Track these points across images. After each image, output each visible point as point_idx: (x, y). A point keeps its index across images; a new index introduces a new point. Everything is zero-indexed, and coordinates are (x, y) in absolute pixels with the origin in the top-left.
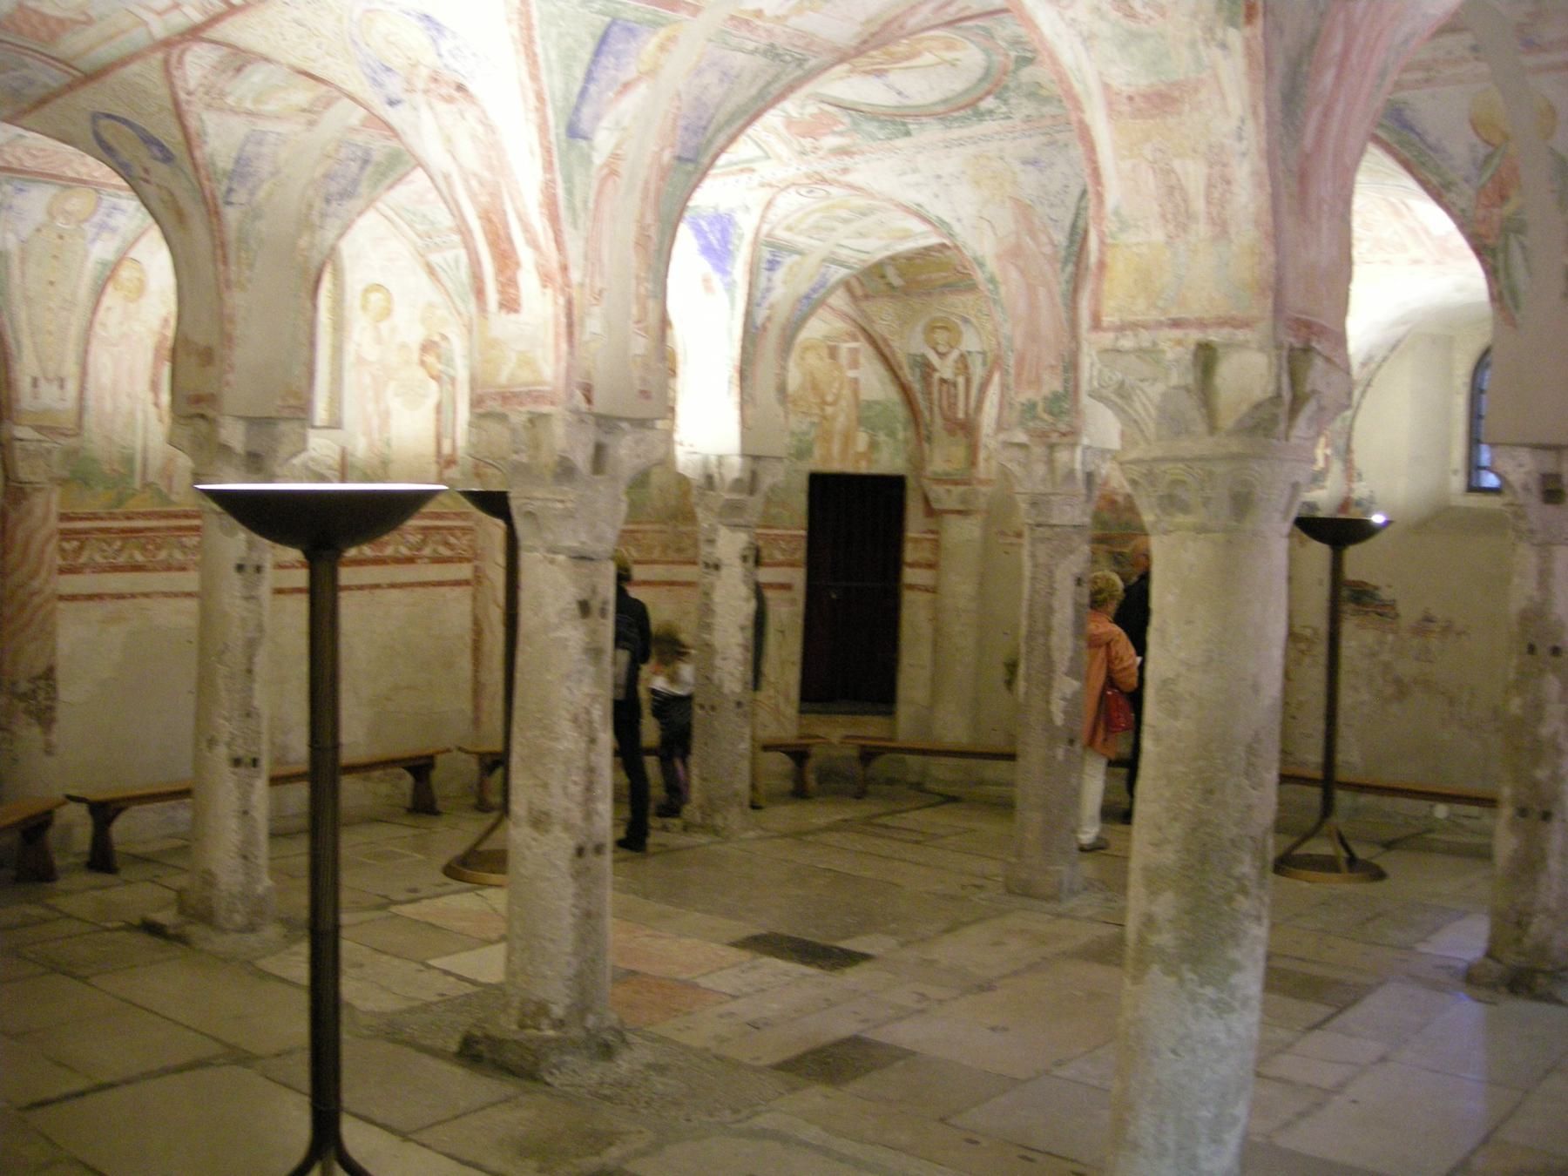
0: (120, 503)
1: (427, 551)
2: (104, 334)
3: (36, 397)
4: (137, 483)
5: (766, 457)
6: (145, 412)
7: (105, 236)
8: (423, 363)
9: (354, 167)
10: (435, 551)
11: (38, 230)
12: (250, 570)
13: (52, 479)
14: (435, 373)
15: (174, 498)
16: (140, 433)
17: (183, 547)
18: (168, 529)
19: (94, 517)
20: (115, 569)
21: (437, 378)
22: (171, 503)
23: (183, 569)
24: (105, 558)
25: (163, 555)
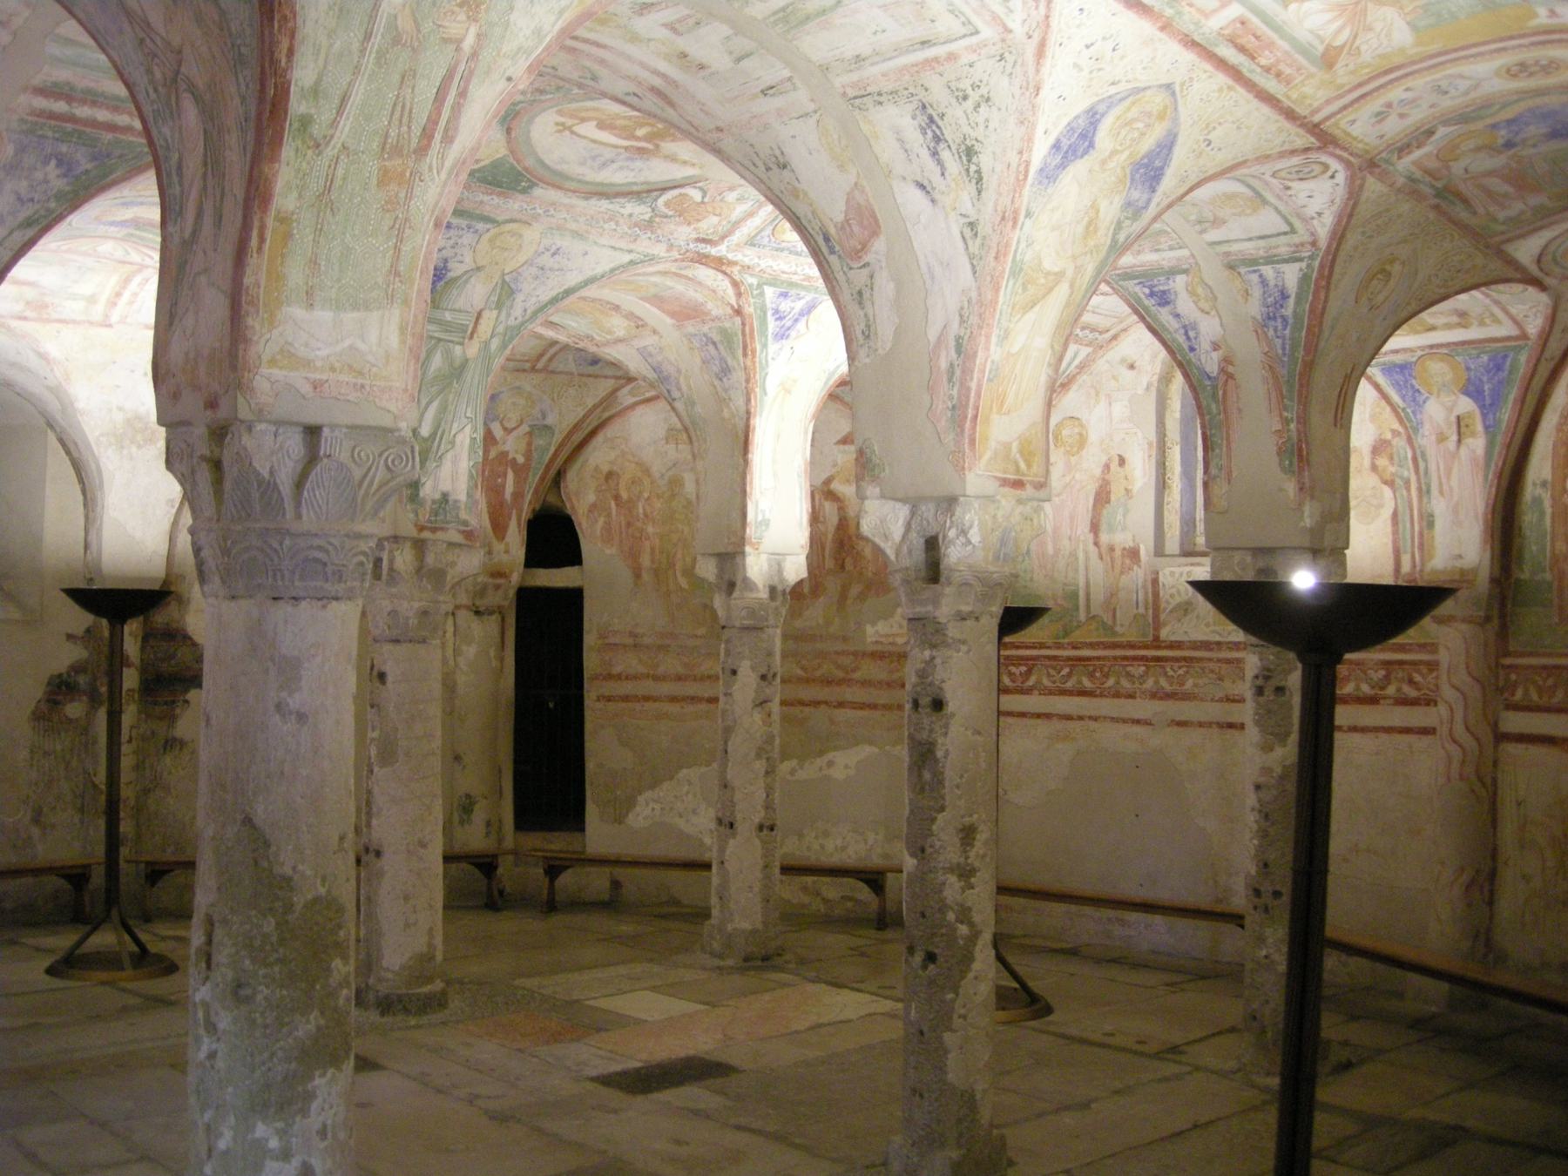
0: (1066, 634)
1: (1391, 690)
4: (1082, 616)
5: (1282, 548)
6: (1086, 553)
8: (1374, 468)
9: (711, 347)
10: (1399, 690)
12: (728, 672)
14: (1387, 477)
15: (1118, 629)
17: (1128, 675)
18: (1115, 658)
19: (1042, 646)
20: (1063, 692)
21: (1390, 483)
22: (1114, 634)
23: (1131, 696)
24: (1054, 682)
25: (1111, 682)
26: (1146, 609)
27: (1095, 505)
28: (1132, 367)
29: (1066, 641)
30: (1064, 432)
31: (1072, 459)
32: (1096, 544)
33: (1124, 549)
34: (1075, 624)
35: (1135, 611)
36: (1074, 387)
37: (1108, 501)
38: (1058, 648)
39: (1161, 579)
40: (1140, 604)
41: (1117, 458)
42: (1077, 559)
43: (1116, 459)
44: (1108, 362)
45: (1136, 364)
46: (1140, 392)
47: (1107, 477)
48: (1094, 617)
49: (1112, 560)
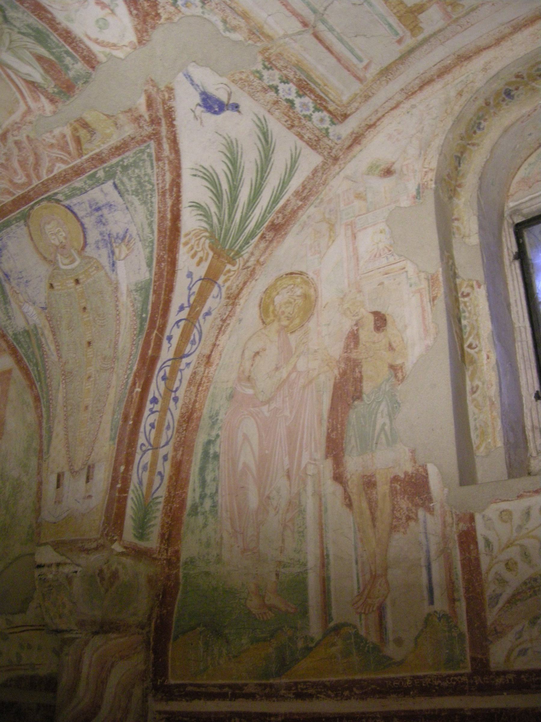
2: (250, 392)
3: (58, 502)
6: (319, 496)
7: (121, 251)
11: (51, 286)
13: (81, 624)
16: (312, 534)
26: (453, 600)
27: (333, 408)
28: (388, 172)
29: (284, 680)
30: (278, 300)
31: (293, 338)
32: (338, 478)
33: (395, 479)
34: (300, 644)
35: (427, 609)
36: (294, 229)
37: (358, 396)
38: (269, 697)
39: (481, 530)
40: (437, 592)
41: (371, 318)
42: (302, 512)
43: (370, 320)
44: (347, 178)
45: (396, 167)
46: (405, 202)
47: (354, 355)
48: (337, 629)
49: (372, 506)
